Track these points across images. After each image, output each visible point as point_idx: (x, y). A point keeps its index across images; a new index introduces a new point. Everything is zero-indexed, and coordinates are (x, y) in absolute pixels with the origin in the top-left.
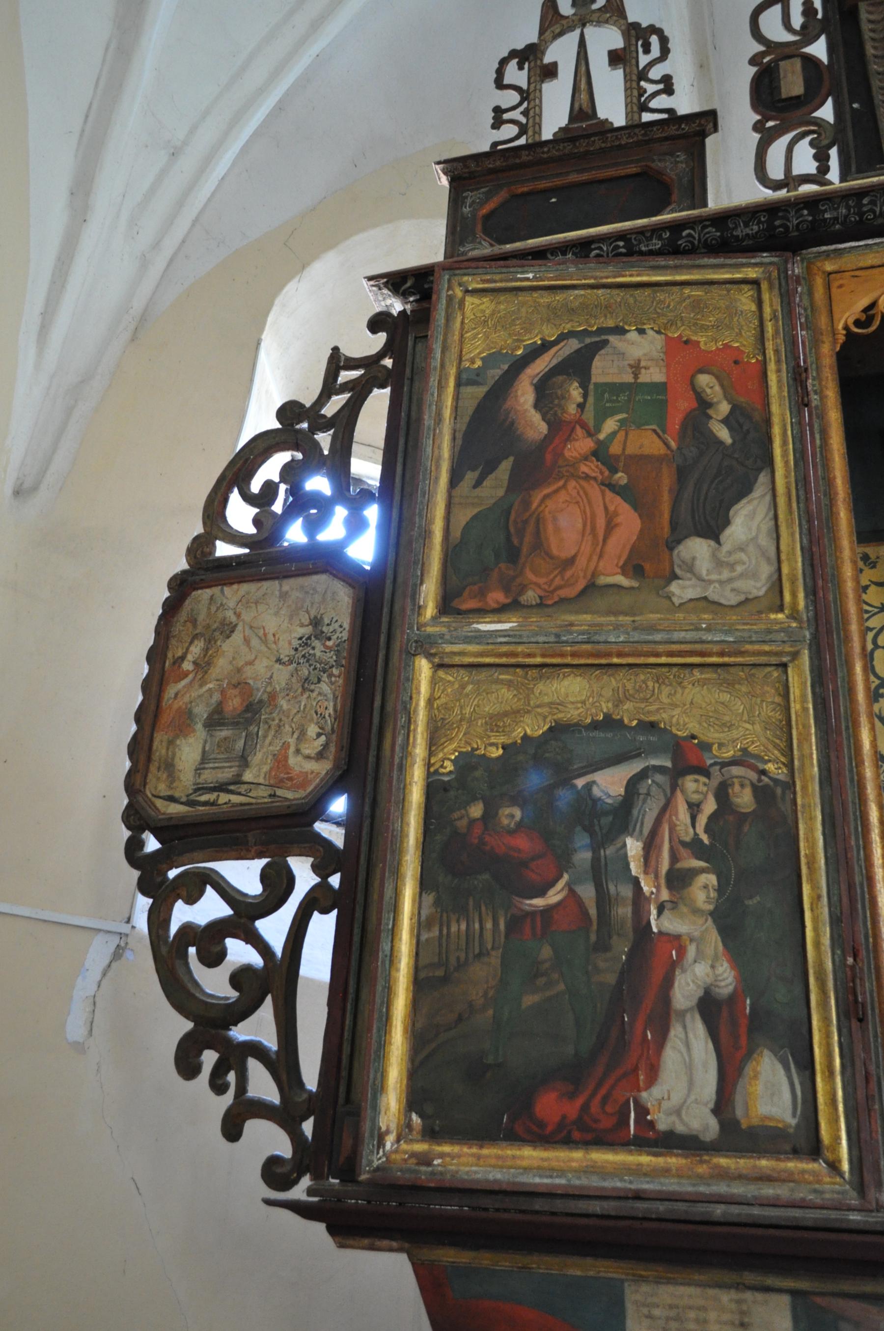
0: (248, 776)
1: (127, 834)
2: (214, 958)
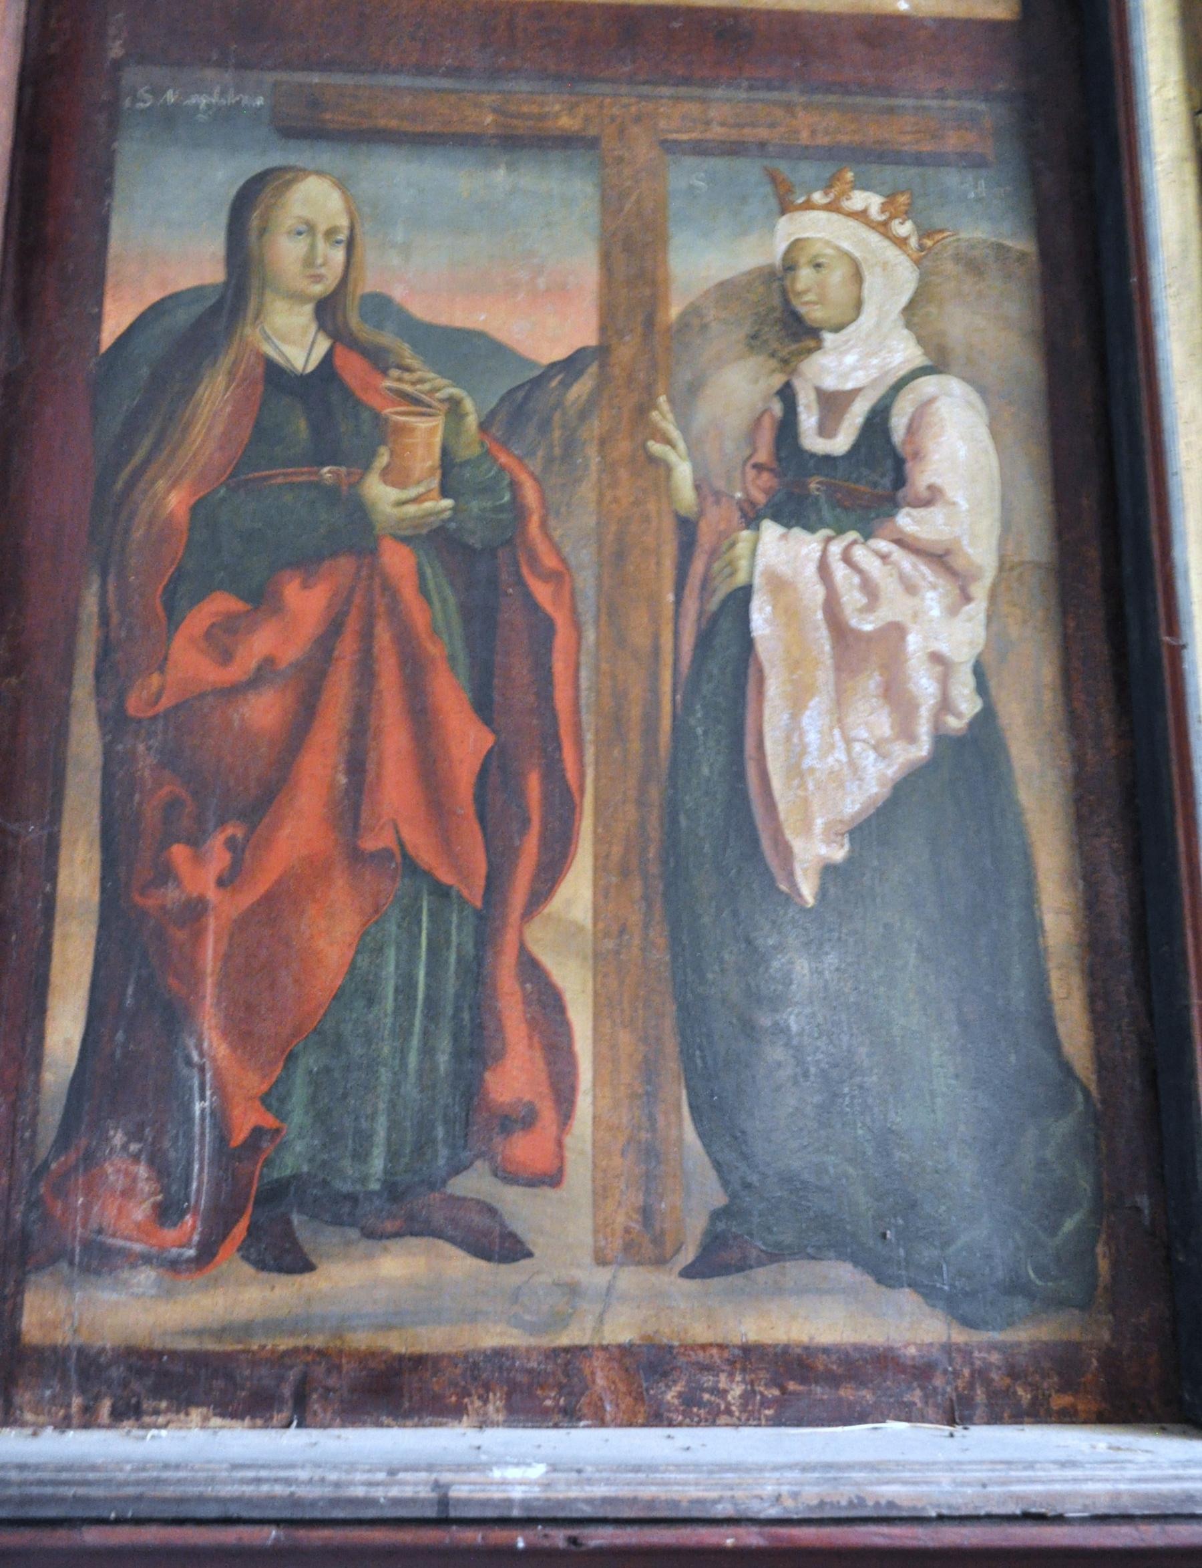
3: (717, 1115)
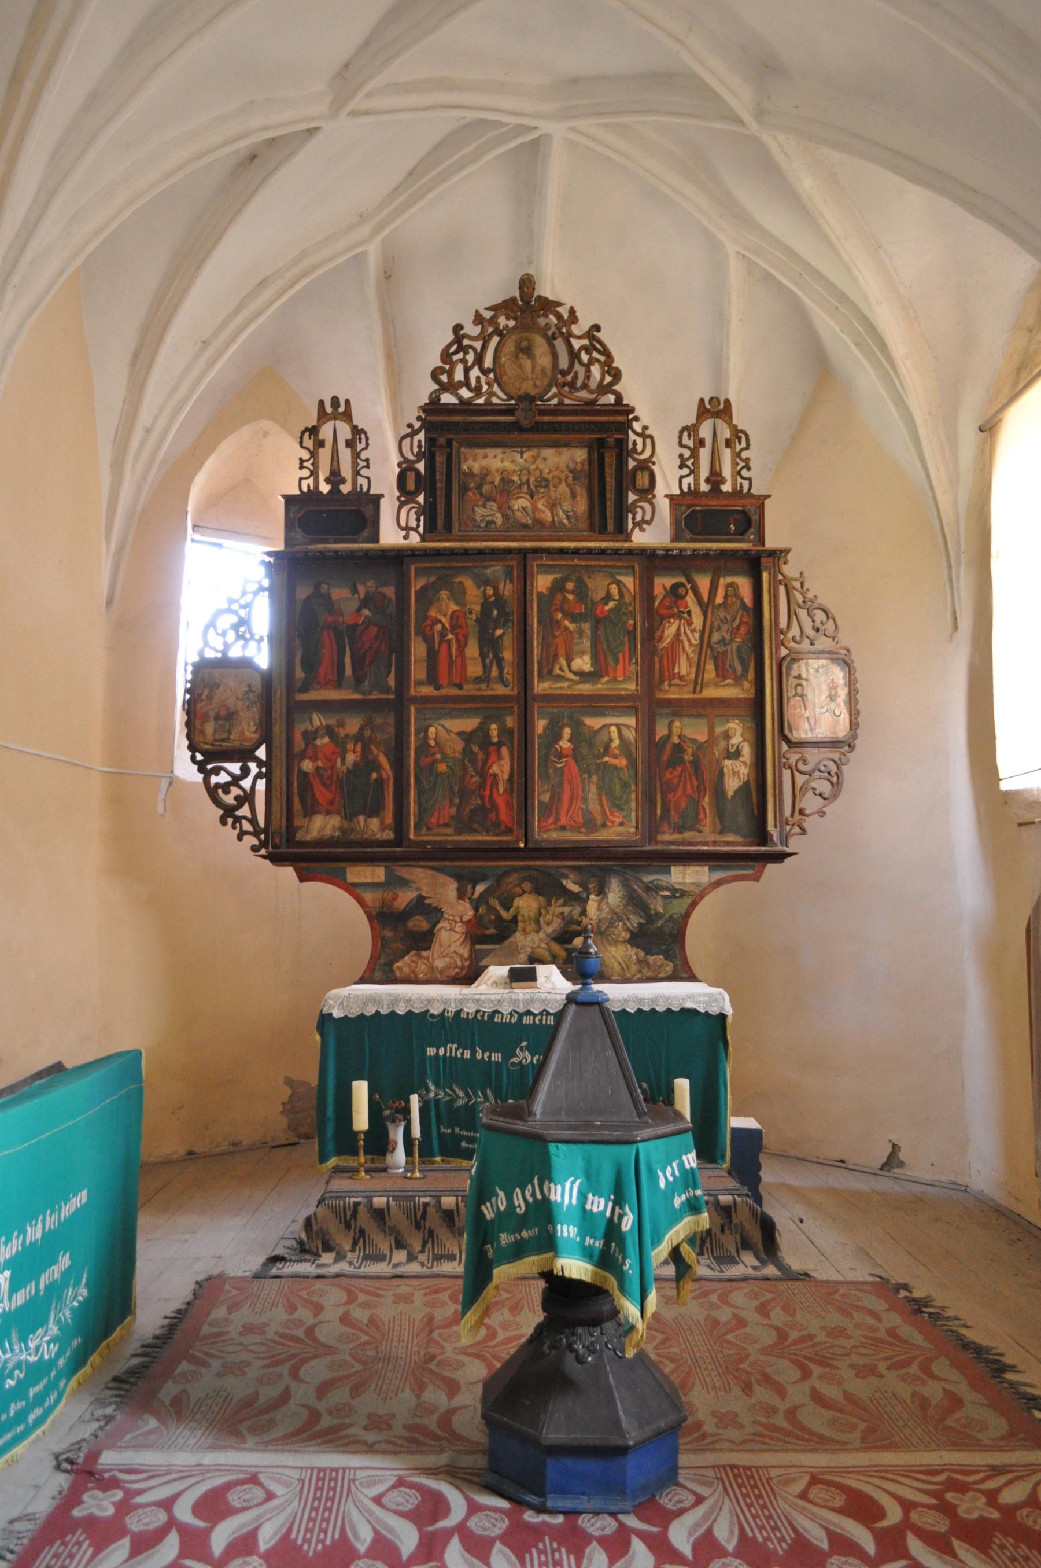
0: (232, 737)
1: (190, 754)
2: (227, 792)
3: (721, 822)
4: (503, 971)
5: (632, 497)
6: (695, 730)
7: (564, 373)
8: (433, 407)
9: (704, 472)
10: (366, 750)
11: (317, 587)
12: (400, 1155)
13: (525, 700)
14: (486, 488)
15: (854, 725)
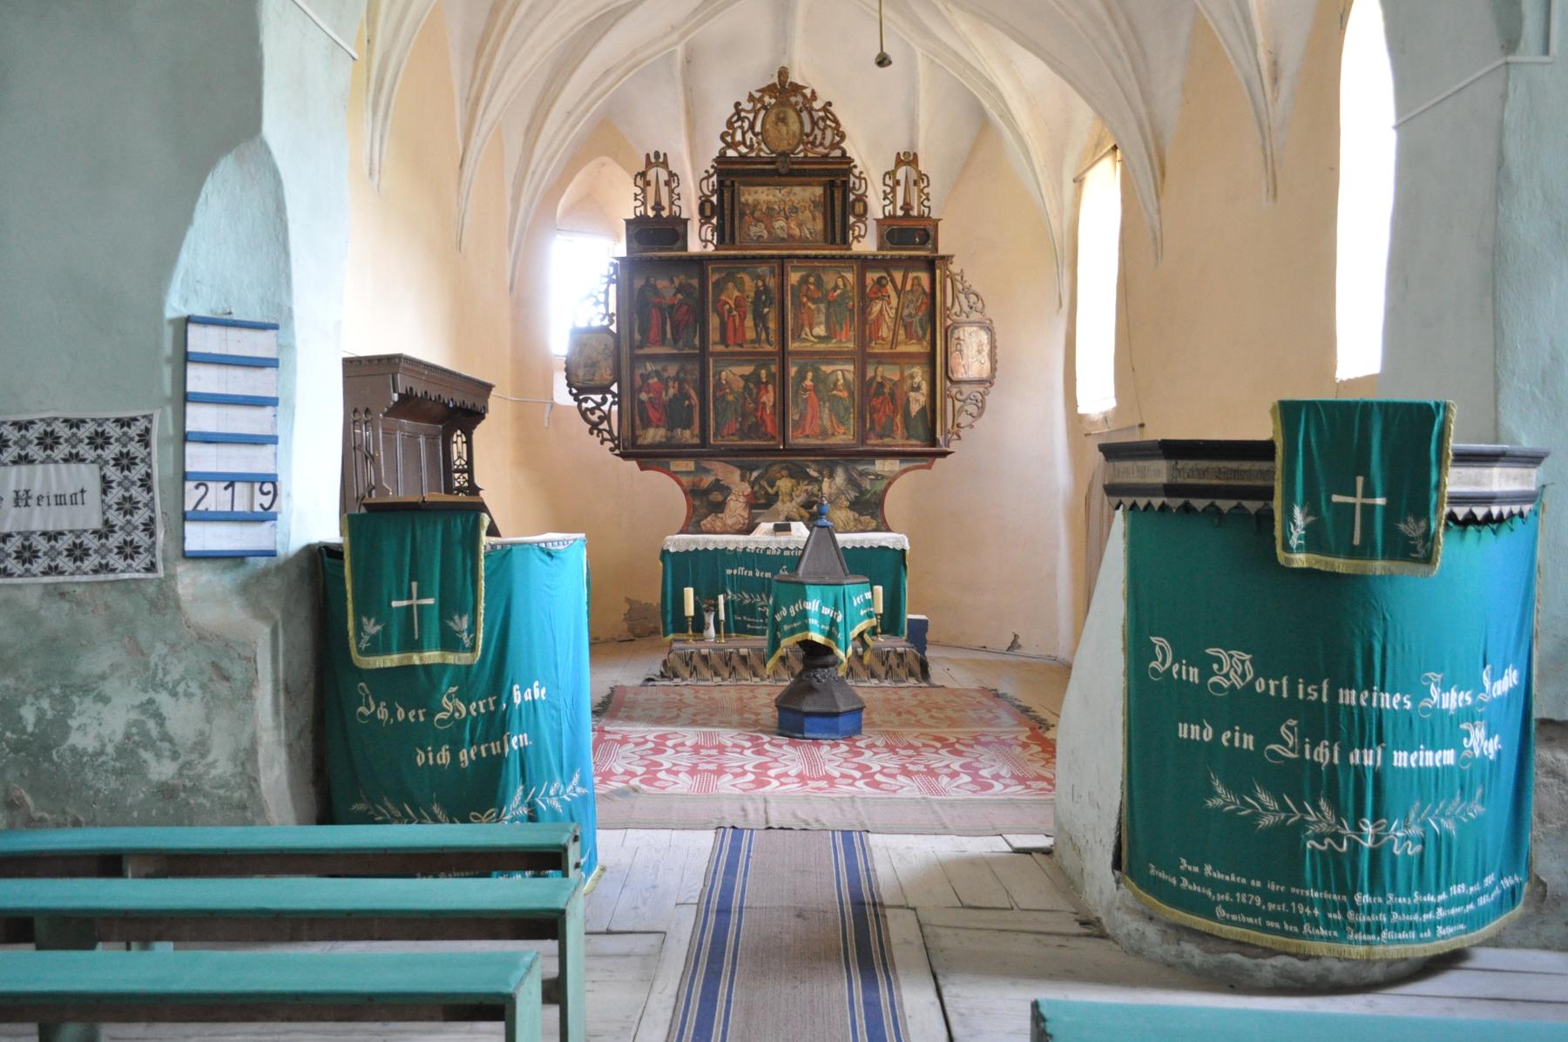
4: (771, 525)
5: (852, 220)
6: (891, 373)
7: (808, 135)
8: (722, 159)
9: (900, 203)
10: (681, 388)
11: (648, 279)
12: (712, 631)
13: (783, 354)
14: (757, 214)
15: (993, 369)
